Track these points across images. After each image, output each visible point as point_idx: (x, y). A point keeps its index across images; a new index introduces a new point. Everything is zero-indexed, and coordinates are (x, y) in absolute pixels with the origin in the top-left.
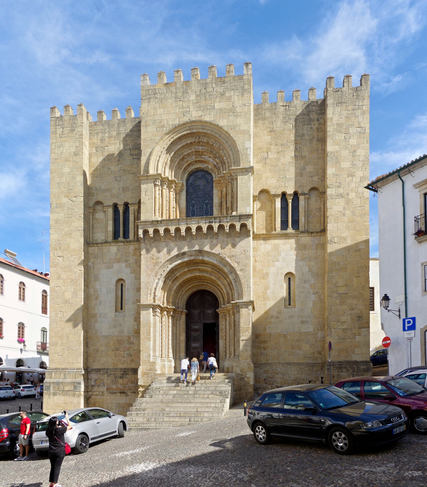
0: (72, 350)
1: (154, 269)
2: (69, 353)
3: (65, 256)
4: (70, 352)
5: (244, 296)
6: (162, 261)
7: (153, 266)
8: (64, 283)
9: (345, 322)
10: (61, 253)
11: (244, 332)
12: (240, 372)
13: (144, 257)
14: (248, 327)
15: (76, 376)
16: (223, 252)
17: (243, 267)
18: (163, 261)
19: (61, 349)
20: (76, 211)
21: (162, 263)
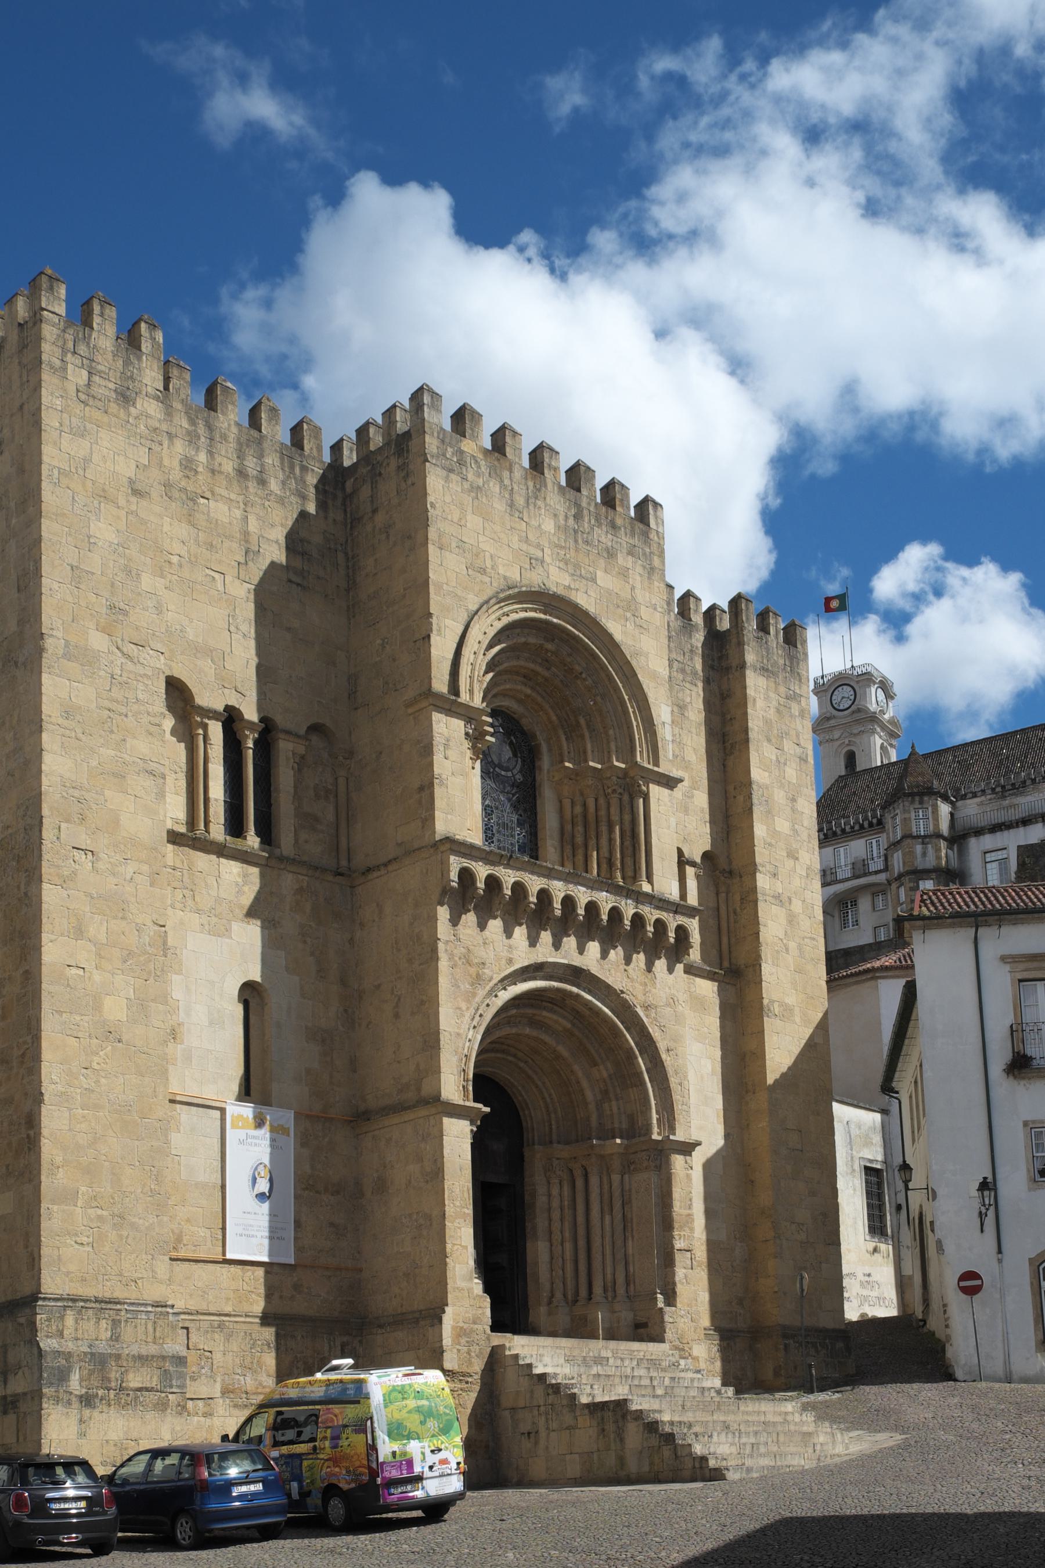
0: (133, 1226)
1: (474, 995)
2: (121, 1237)
3: (102, 855)
4: (125, 1233)
5: (677, 1126)
6: (495, 976)
7: (469, 983)
8: (101, 957)
9: (803, 1224)
10: (84, 836)
11: (681, 1228)
12: (677, 1343)
13: (446, 950)
14: (689, 1215)
15: (158, 1334)
16: (631, 990)
17: (671, 1045)
18: (497, 978)
19: (91, 1220)
20: (140, 696)
21: (492, 984)
